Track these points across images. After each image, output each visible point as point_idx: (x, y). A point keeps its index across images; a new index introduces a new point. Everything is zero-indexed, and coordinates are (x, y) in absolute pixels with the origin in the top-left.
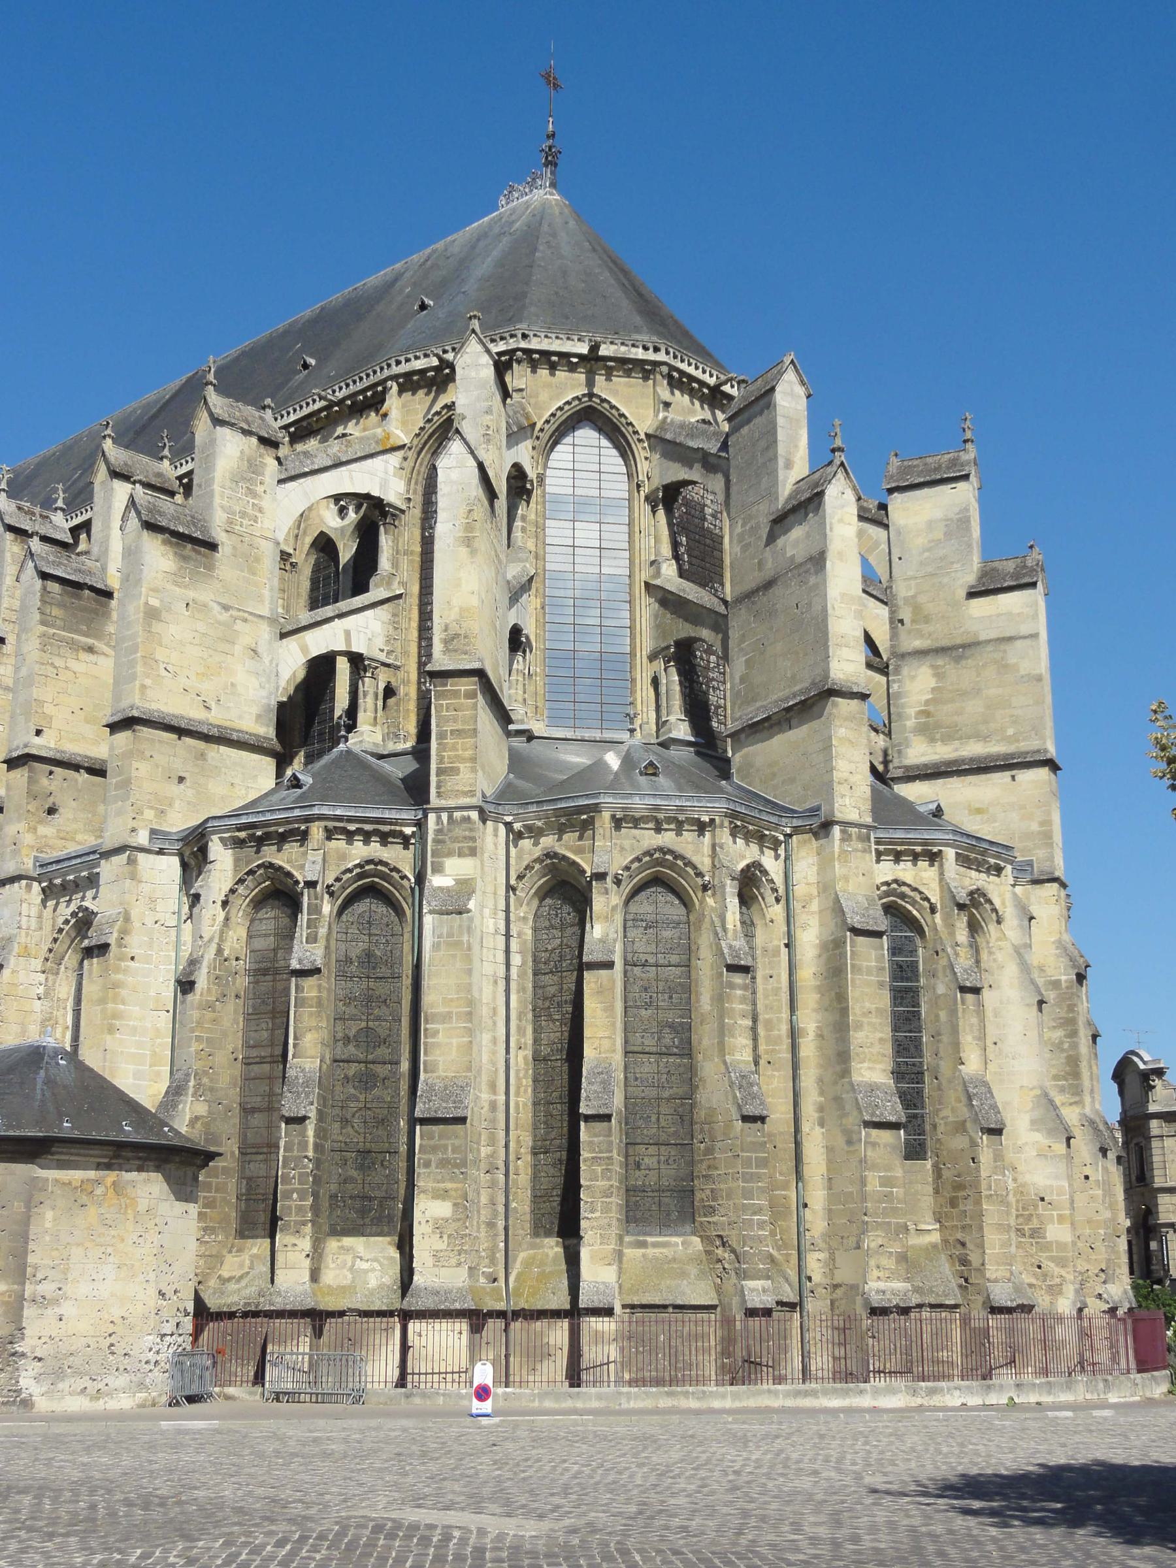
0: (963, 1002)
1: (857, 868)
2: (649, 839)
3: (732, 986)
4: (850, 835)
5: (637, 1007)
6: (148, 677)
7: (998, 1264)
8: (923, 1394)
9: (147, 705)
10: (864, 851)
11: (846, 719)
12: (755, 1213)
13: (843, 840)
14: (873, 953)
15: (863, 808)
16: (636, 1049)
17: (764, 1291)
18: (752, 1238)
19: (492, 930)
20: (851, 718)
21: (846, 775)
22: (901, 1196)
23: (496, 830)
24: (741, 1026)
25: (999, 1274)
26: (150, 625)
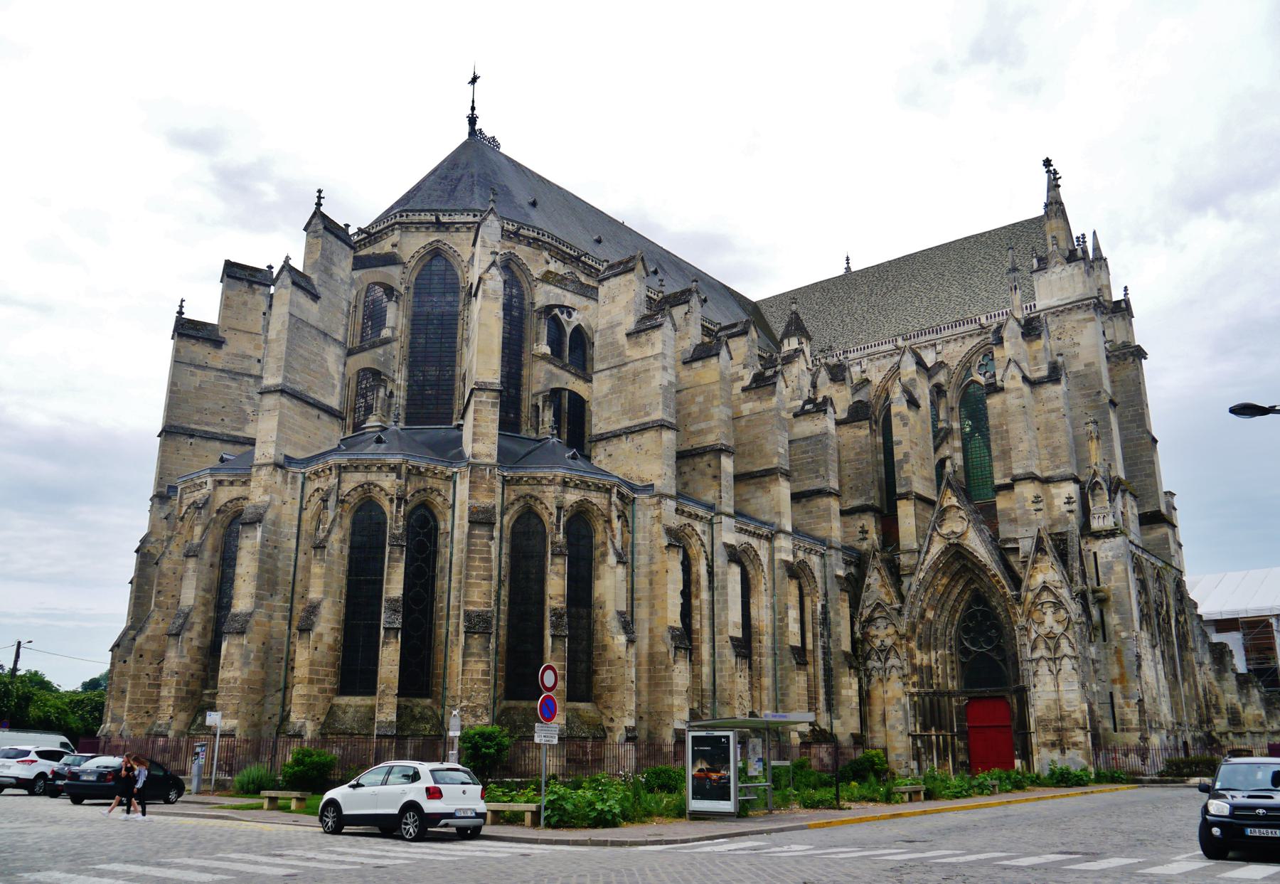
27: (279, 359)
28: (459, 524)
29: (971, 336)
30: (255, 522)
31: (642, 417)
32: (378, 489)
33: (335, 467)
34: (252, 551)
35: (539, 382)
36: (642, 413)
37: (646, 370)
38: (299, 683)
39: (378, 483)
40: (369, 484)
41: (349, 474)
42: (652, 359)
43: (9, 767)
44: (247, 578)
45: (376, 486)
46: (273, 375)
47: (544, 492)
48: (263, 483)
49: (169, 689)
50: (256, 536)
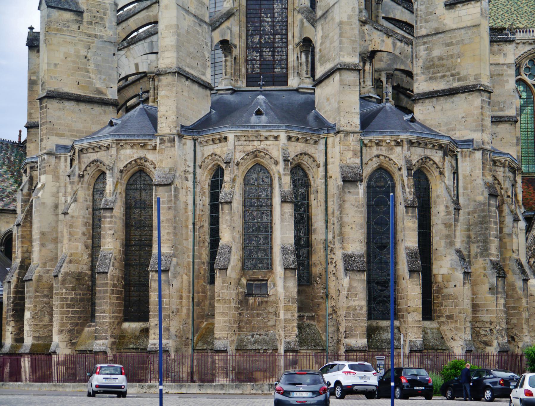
0: (222, 210)
1: (167, 155)
2: (93, 156)
3: (105, 217)
4: (165, 141)
5: (97, 228)
6: (32, 109)
7: (221, 331)
8: (146, 388)
9: (33, 121)
10: (171, 146)
11: (165, 87)
12: (101, 313)
13: (161, 143)
14: (166, 194)
15: (172, 127)
16: (96, 245)
17: (103, 344)
18: (100, 323)
19: (63, 201)
20: (167, 86)
21: (164, 113)
22: (168, 302)
23: (66, 160)
24: (108, 234)
25: (221, 336)
26: (32, 88)
27: (354, 42)
28: (463, 193)
29: (524, 43)
30: (357, 181)
31: (496, 111)
32: (431, 162)
33: (407, 142)
34: (357, 204)
35: (382, 60)
36: (497, 108)
37: (499, 75)
38: (414, 312)
39: (432, 157)
40: (427, 158)
41: (414, 148)
42: (505, 67)
43: (369, 378)
44: (354, 226)
45: (431, 160)
46: (349, 54)
47: (497, 171)
48: (352, 148)
49: (292, 313)
50: (358, 194)
